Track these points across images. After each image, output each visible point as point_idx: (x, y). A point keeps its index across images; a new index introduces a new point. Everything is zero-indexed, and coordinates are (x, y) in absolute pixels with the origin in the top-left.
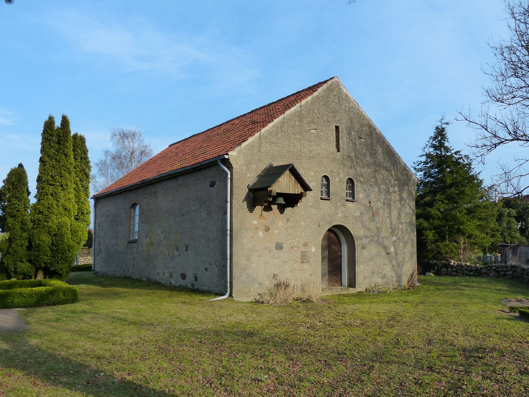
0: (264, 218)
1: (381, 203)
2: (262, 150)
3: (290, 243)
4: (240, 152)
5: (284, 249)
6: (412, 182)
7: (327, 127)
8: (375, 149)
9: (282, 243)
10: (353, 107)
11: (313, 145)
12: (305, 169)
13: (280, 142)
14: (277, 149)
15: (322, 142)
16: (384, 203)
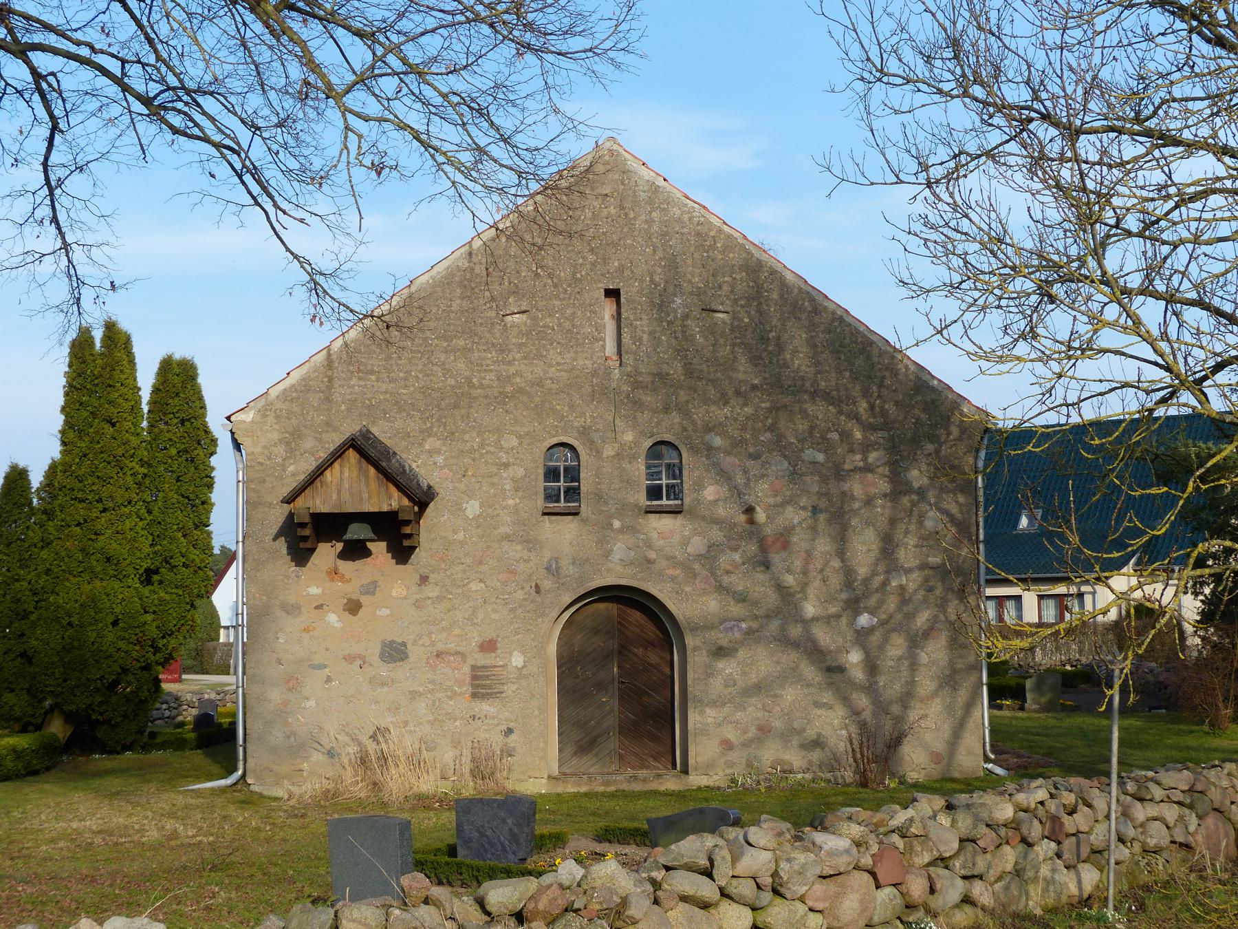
0: (343, 579)
1: (804, 508)
2: (337, 398)
3: (433, 644)
4: (266, 410)
5: (411, 659)
6: (955, 431)
7: (570, 299)
8: (779, 338)
9: (404, 644)
10: (679, 220)
11: (514, 360)
12: (485, 432)
13: (395, 367)
14: (384, 387)
15: (551, 344)
16: (815, 510)
